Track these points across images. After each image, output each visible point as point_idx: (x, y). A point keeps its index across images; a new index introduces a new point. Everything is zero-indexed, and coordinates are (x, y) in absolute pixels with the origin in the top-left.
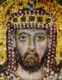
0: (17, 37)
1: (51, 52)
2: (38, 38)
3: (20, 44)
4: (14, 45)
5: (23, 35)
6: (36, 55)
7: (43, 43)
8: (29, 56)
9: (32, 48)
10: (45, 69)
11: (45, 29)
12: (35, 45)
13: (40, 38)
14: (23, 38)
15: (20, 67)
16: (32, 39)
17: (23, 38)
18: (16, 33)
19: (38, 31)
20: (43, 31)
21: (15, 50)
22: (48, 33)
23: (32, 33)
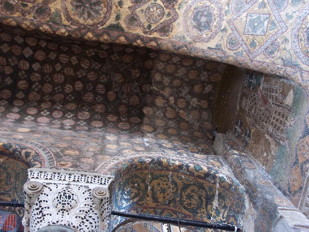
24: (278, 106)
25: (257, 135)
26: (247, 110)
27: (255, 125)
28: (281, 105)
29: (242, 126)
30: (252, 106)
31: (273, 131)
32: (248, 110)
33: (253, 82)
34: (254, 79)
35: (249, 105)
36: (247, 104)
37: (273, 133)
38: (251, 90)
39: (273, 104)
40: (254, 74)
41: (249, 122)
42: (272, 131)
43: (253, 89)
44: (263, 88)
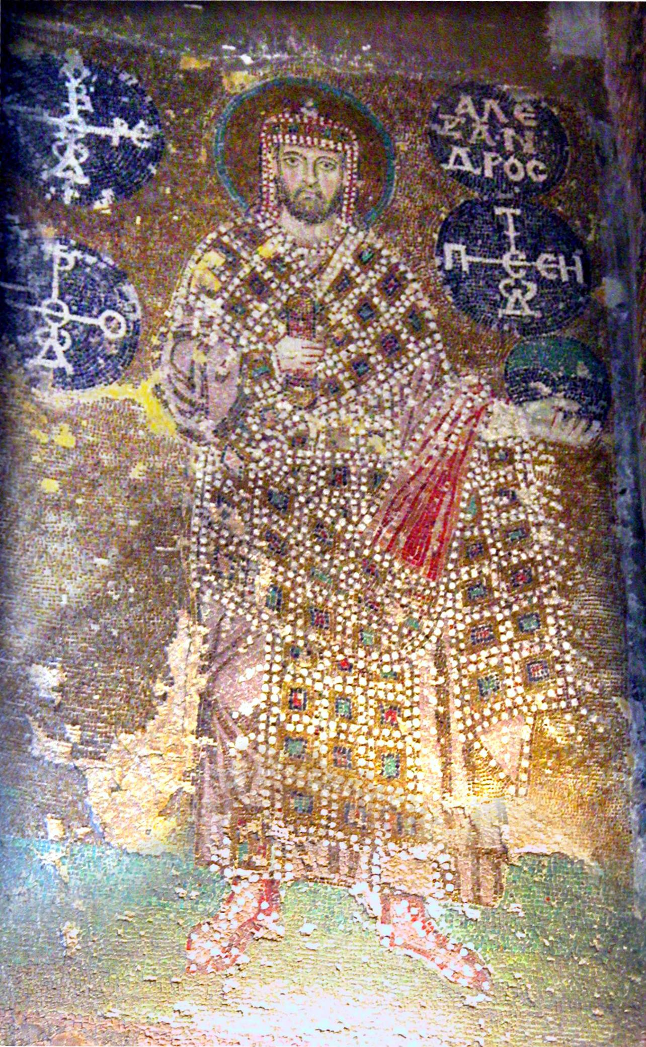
0: (281, 158)
1: (349, 193)
2: (322, 166)
3: (286, 172)
4: (274, 172)
5: (292, 156)
6: (319, 195)
7: (334, 176)
8: (303, 195)
9: (311, 180)
10: (338, 221)
11: (336, 151)
12: (315, 175)
13: (326, 166)
14: (293, 161)
15: (285, 214)
16: (310, 167)
17: (293, 161)
18: (278, 149)
19: (324, 154)
20: (332, 155)
21: (275, 180)
22: (343, 160)
23: (311, 155)
24: (442, 722)
25: (134, 487)
26: (267, 250)
27: (206, 426)
28: (458, 767)
29: (122, 191)
30: (320, 312)
31: (250, 725)
32: (275, 262)
33: (506, 261)
34: (540, 281)
35: (321, 269)
36: (312, 219)
37: (232, 736)
38: (441, 253)
39: (440, 661)
40: (570, 262)
41: (189, 310)
42: (246, 709)
43: (454, 278)
44: (508, 457)
